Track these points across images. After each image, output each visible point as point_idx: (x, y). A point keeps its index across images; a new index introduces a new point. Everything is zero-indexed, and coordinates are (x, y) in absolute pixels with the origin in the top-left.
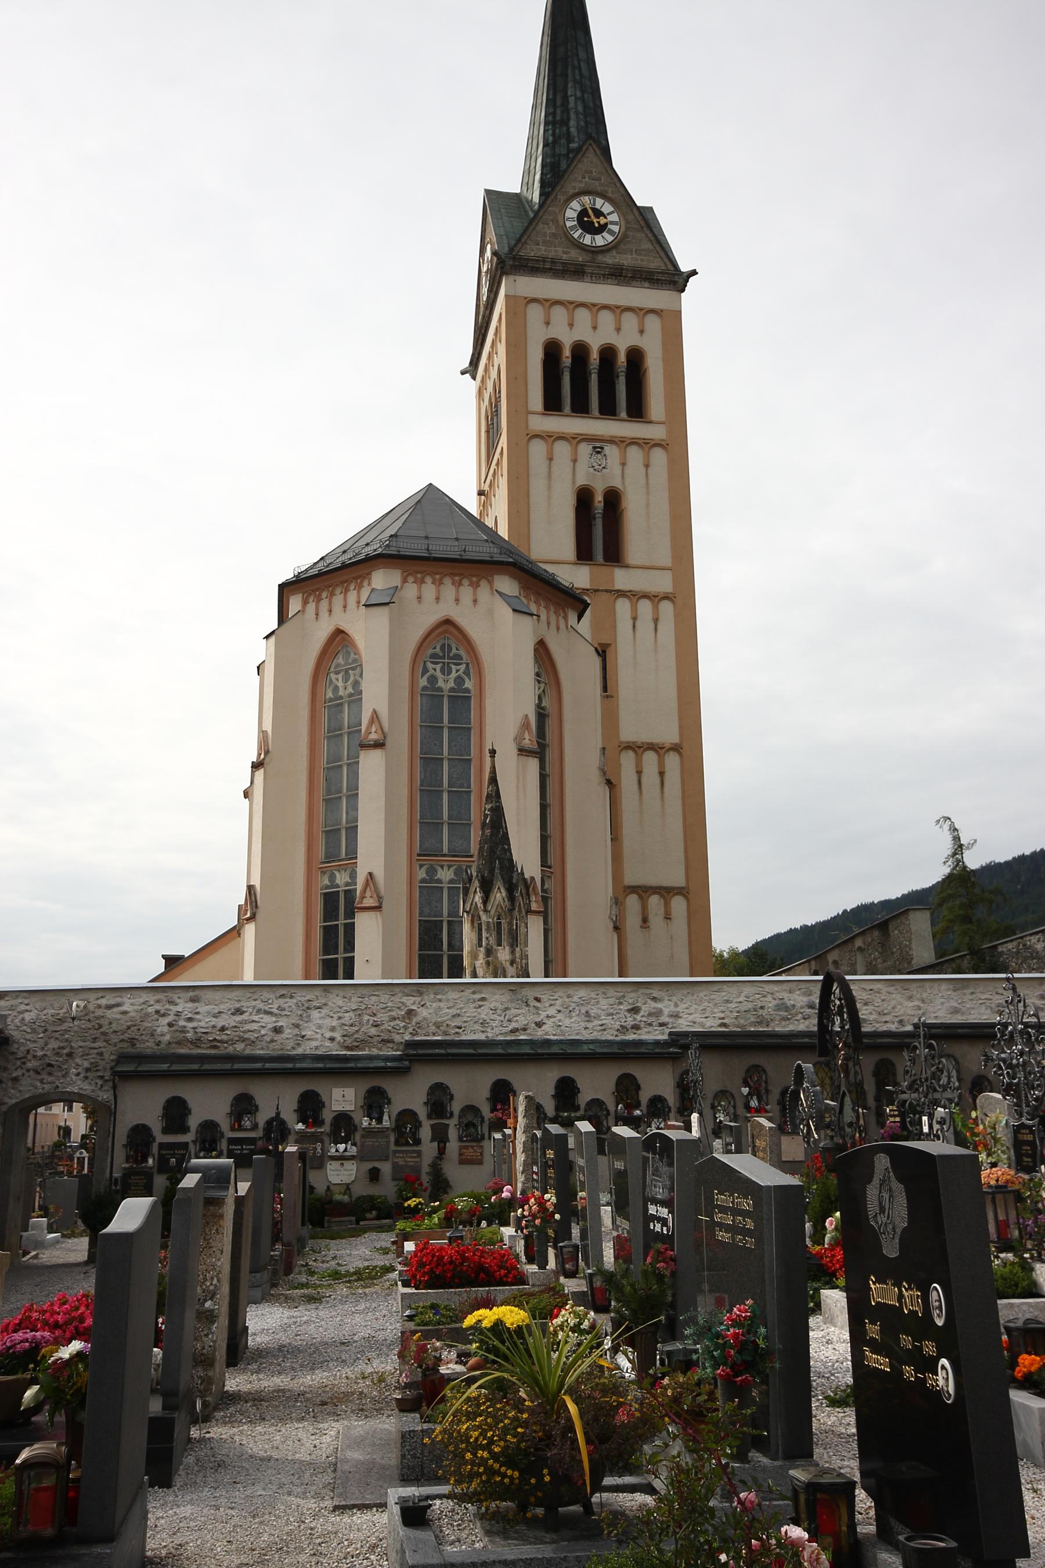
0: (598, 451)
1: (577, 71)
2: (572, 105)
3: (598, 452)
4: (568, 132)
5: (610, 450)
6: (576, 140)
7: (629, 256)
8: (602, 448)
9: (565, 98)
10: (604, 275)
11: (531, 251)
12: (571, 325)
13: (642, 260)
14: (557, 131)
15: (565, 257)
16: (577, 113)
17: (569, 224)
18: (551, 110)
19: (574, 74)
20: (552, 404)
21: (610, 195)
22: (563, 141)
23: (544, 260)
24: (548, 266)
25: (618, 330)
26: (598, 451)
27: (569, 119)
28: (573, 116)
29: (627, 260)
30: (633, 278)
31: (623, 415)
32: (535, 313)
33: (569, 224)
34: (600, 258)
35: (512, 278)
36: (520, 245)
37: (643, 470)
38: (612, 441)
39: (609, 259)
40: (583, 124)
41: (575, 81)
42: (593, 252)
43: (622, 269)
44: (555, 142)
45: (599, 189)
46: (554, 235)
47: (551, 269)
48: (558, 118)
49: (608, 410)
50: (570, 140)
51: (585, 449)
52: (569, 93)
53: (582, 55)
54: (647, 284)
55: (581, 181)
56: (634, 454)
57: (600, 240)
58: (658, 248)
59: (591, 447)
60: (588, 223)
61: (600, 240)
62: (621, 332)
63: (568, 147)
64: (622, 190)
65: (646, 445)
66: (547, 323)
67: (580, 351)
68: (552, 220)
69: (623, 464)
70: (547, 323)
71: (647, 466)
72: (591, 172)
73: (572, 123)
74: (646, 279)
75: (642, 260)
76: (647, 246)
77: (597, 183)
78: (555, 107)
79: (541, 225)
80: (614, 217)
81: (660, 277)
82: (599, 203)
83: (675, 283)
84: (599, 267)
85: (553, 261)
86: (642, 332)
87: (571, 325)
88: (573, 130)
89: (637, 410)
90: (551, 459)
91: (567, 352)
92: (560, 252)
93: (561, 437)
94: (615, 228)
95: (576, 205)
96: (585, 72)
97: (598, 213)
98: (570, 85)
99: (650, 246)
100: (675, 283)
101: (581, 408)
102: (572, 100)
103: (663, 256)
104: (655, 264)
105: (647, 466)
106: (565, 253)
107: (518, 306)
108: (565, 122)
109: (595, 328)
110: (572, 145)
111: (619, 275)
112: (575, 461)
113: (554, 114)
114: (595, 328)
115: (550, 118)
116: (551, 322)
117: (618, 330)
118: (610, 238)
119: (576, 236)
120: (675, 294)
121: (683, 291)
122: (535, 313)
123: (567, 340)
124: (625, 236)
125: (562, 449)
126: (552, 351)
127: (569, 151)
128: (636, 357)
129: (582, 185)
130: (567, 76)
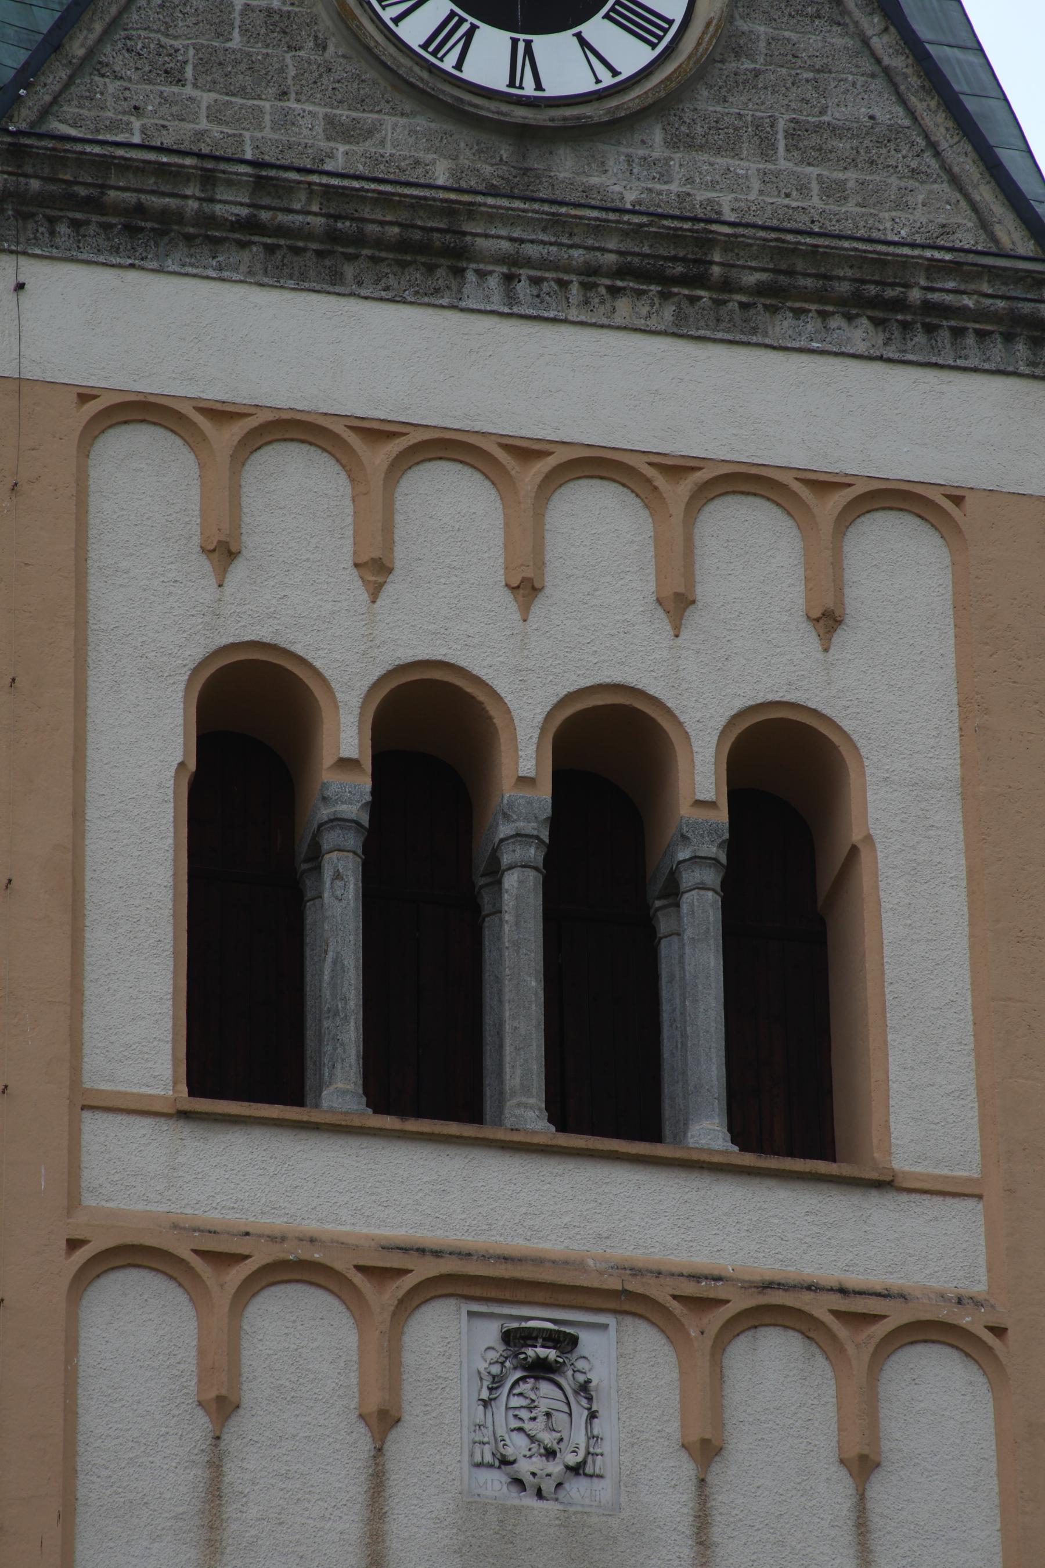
0: (538, 1357)
3: (541, 1370)
5: (606, 1351)
7: (748, 166)
8: (566, 1342)
12: (376, 570)
13: (834, 191)
15: (341, 157)
20: (241, 1050)
23: (210, 168)
24: (231, 204)
25: (678, 604)
26: (538, 1357)
29: (733, 185)
30: (775, 296)
31: (709, 1132)
32: (143, 488)
34: (566, 168)
36: (56, 76)
37: (835, 1490)
38: (628, 1297)
39: (619, 178)
42: (524, 135)
43: (706, 242)
47: (250, 226)
49: (608, 1098)
51: (452, 1345)
54: (860, 335)
56: (777, 1382)
58: (938, 124)
59: (490, 1333)
62: (694, 618)
65: (856, 1327)
66: (223, 553)
67: (432, 728)
69: (706, 1451)
70: (223, 553)
71: (863, 1466)
74: (853, 306)
75: (834, 191)
76: (862, 104)
81: (946, 292)
85: (266, 179)
86: (828, 621)
87: (376, 570)
89: (797, 1107)
90: (223, 1407)
91: (345, 735)
92: (302, 125)
93: (300, 1267)
99: (887, 112)
101: (428, 1079)
103: (968, 166)
105: (863, 1466)
106: (337, 130)
109: (527, 589)
111: (688, 275)
112: (383, 1420)
114: (527, 589)
116: (251, 542)
117: (678, 604)
118: (630, 55)
122: (143, 488)
123: (348, 657)
124: (727, 42)
125: (301, 1342)
126: (247, 727)
128: (789, 774)
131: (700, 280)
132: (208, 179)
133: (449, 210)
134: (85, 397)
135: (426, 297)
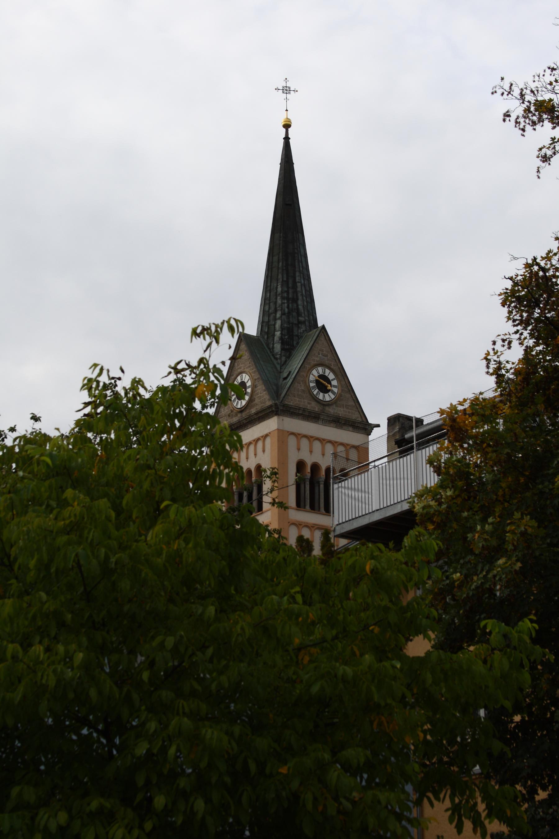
1: (300, 264)
2: (299, 289)
4: (298, 309)
6: (303, 315)
7: (342, 409)
9: (295, 282)
10: (329, 420)
11: (293, 401)
13: (349, 412)
14: (290, 305)
16: (302, 295)
17: (312, 385)
18: (286, 289)
19: (299, 264)
21: (332, 367)
22: (294, 314)
27: (298, 299)
28: (300, 297)
29: (340, 411)
30: (344, 424)
32: (292, 441)
33: (312, 385)
34: (327, 408)
35: (281, 418)
39: (332, 410)
40: (305, 303)
41: (300, 272)
42: (324, 405)
43: (340, 419)
44: (289, 313)
45: (327, 362)
46: (303, 391)
47: (302, 414)
48: (290, 296)
50: (299, 314)
52: (297, 280)
53: (302, 251)
54: (351, 429)
55: (317, 356)
57: (328, 397)
60: (323, 385)
61: (328, 397)
63: (298, 320)
64: (339, 365)
67: (315, 467)
68: (302, 381)
70: (299, 449)
72: (322, 351)
73: (300, 302)
75: (349, 412)
76: (351, 403)
77: (326, 358)
78: (288, 287)
79: (296, 384)
80: (334, 383)
82: (327, 371)
83: (366, 429)
84: (328, 416)
85: (304, 410)
88: (300, 307)
94: (335, 390)
95: (314, 372)
96: (304, 265)
97: (329, 382)
98: (297, 274)
99: (354, 404)
100: (366, 429)
102: (299, 285)
104: (355, 416)
106: (309, 403)
107: (283, 436)
108: (295, 300)
110: (300, 318)
113: (288, 292)
115: (285, 295)
119: (315, 393)
120: (366, 436)
121: (370, 434)
122: (292, 441)
124: (341, 395)
127: (299, 322)
129: (318, 359)
130: (295, 267)
131: (338, 422)
132: (299, 409)
133: (319, 414)
134: (288, 432)
135: (316, 422)
